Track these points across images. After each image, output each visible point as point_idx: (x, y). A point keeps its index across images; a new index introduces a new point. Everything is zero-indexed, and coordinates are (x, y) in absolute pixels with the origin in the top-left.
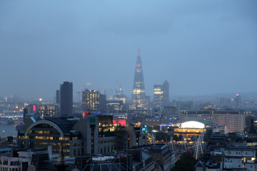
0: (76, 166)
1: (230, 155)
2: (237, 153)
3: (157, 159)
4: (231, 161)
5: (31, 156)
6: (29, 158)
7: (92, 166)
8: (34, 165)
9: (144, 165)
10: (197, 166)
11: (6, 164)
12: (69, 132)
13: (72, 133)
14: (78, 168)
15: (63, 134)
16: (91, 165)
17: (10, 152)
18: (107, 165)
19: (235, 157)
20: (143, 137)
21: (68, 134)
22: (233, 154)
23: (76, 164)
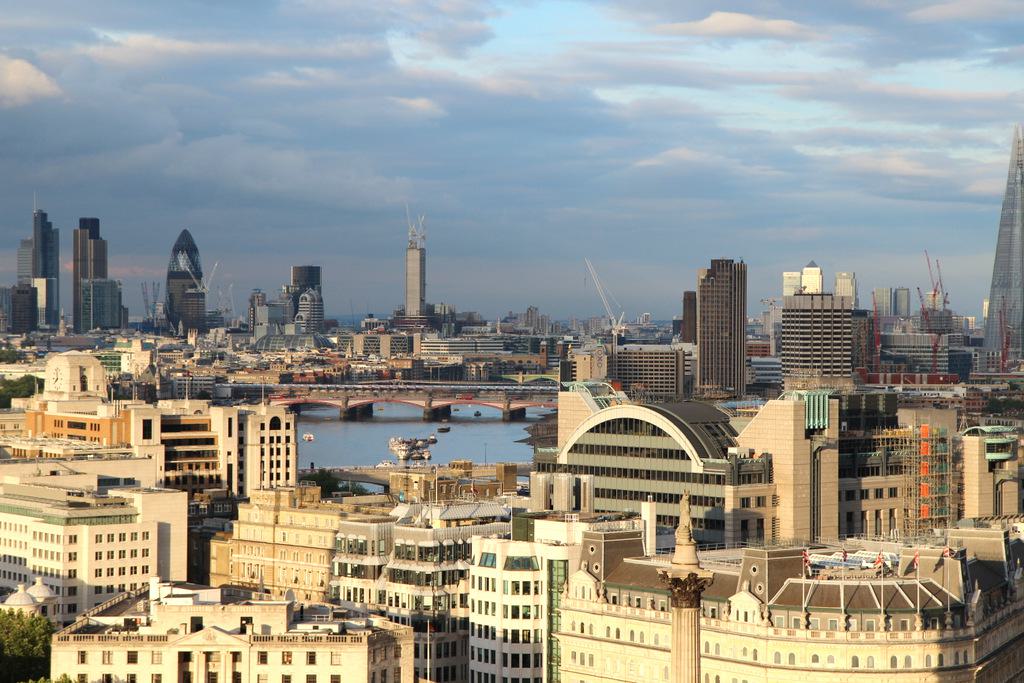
5: (579, 540)
11: (489, 563)
15: (698, 459)
16: (803, 580)
17: (504, 519)
18: (866, 587)
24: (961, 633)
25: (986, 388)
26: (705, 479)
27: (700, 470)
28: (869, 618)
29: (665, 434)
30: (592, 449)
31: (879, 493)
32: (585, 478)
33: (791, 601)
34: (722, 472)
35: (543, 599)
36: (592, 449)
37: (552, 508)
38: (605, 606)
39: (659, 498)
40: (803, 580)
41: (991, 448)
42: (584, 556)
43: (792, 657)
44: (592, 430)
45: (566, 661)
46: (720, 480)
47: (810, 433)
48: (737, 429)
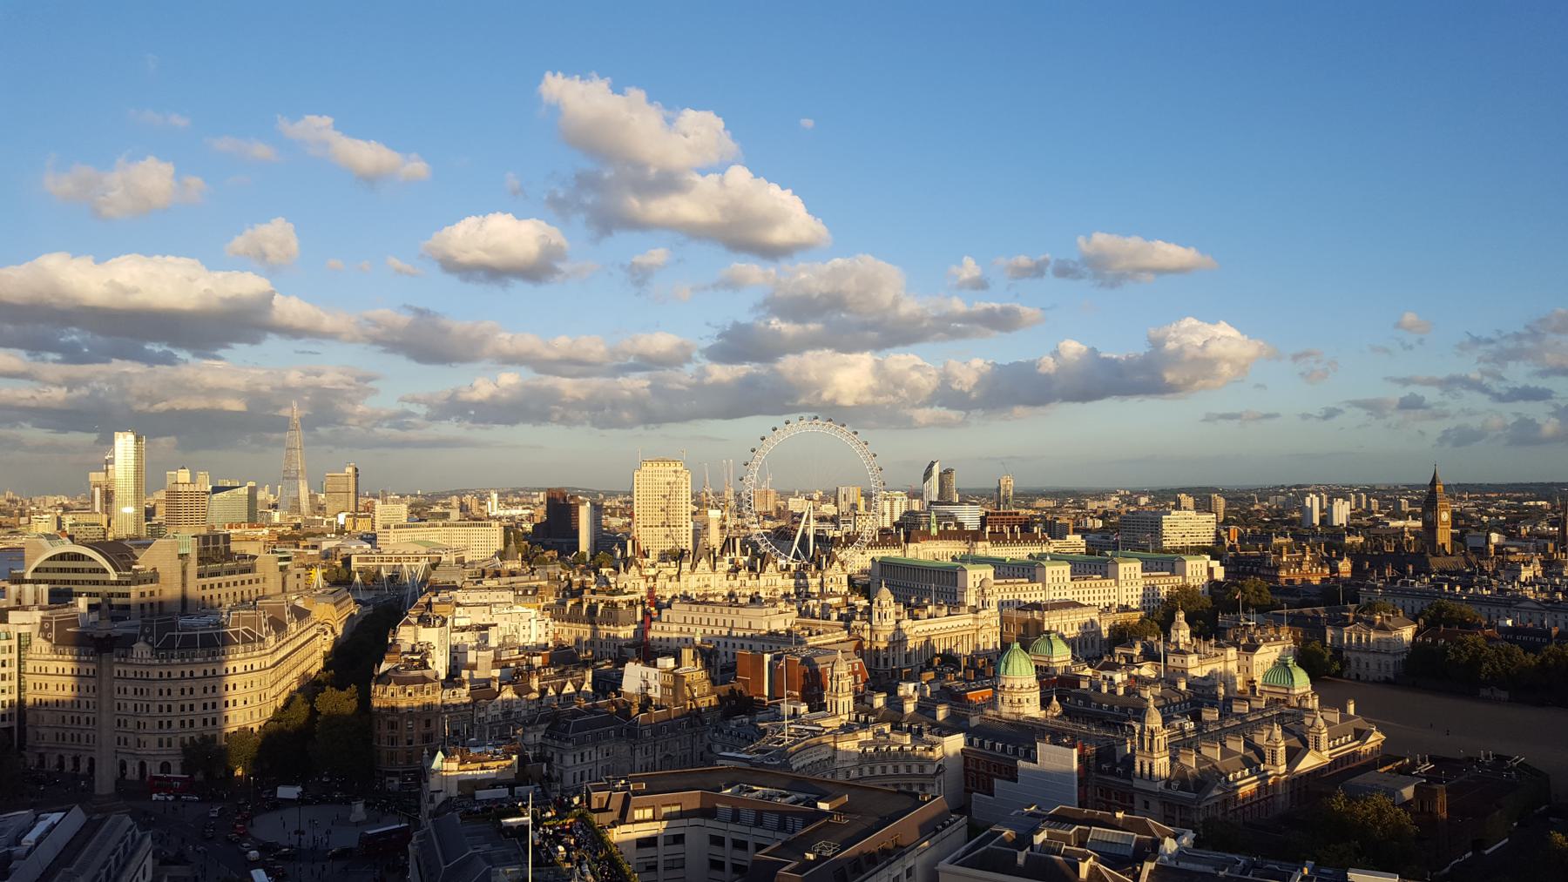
0: (142, 638)
1: (468, 601)
2: (481, 597)
3: (324, 617)
4: (470, 612)
5: (38, 620)
6: (35, 623)
7: (178, 636)
8: (45, 638)
9: (294, 630)
10: (403, 625)
12: (130, 569)
13: (135, 570)
14: (146, 641)
16: (176, 633)
19: (477, 605)
20: (296, 576)
21: (127, 573)
22: (475, 597)
23: (142, 633)
24: (263, 652)
25: (280, 530)
26: (118, 583)
27: (116, 579)
28: (212, 650)
29: (94, 560)
30: (47, 570)
31: (220, 585)
32: (42, 586)
33: (168, 645)
34: (128, 579)
35: (15, 656)
36: (47, 570)
37: (20, 604)
38: (55, 657)
39: (89, 595)
40: (176, 633)
41: (281, 559)
42: (42, 629)
43: (169, 674)
44: (47, 560)
45: (30, 688)
46: (128, 583)
47: (181, 556)
48: (138, 556)
